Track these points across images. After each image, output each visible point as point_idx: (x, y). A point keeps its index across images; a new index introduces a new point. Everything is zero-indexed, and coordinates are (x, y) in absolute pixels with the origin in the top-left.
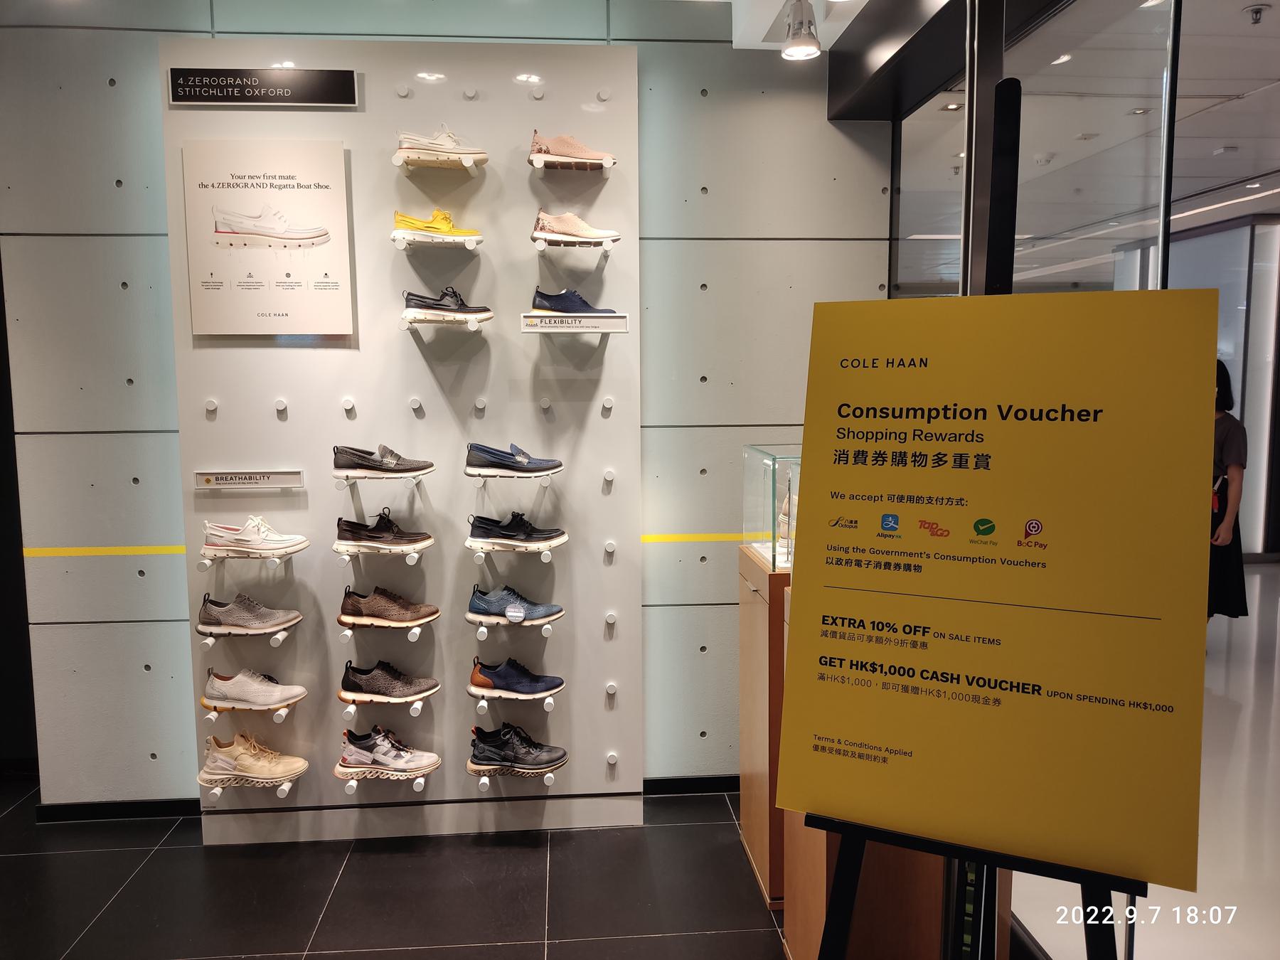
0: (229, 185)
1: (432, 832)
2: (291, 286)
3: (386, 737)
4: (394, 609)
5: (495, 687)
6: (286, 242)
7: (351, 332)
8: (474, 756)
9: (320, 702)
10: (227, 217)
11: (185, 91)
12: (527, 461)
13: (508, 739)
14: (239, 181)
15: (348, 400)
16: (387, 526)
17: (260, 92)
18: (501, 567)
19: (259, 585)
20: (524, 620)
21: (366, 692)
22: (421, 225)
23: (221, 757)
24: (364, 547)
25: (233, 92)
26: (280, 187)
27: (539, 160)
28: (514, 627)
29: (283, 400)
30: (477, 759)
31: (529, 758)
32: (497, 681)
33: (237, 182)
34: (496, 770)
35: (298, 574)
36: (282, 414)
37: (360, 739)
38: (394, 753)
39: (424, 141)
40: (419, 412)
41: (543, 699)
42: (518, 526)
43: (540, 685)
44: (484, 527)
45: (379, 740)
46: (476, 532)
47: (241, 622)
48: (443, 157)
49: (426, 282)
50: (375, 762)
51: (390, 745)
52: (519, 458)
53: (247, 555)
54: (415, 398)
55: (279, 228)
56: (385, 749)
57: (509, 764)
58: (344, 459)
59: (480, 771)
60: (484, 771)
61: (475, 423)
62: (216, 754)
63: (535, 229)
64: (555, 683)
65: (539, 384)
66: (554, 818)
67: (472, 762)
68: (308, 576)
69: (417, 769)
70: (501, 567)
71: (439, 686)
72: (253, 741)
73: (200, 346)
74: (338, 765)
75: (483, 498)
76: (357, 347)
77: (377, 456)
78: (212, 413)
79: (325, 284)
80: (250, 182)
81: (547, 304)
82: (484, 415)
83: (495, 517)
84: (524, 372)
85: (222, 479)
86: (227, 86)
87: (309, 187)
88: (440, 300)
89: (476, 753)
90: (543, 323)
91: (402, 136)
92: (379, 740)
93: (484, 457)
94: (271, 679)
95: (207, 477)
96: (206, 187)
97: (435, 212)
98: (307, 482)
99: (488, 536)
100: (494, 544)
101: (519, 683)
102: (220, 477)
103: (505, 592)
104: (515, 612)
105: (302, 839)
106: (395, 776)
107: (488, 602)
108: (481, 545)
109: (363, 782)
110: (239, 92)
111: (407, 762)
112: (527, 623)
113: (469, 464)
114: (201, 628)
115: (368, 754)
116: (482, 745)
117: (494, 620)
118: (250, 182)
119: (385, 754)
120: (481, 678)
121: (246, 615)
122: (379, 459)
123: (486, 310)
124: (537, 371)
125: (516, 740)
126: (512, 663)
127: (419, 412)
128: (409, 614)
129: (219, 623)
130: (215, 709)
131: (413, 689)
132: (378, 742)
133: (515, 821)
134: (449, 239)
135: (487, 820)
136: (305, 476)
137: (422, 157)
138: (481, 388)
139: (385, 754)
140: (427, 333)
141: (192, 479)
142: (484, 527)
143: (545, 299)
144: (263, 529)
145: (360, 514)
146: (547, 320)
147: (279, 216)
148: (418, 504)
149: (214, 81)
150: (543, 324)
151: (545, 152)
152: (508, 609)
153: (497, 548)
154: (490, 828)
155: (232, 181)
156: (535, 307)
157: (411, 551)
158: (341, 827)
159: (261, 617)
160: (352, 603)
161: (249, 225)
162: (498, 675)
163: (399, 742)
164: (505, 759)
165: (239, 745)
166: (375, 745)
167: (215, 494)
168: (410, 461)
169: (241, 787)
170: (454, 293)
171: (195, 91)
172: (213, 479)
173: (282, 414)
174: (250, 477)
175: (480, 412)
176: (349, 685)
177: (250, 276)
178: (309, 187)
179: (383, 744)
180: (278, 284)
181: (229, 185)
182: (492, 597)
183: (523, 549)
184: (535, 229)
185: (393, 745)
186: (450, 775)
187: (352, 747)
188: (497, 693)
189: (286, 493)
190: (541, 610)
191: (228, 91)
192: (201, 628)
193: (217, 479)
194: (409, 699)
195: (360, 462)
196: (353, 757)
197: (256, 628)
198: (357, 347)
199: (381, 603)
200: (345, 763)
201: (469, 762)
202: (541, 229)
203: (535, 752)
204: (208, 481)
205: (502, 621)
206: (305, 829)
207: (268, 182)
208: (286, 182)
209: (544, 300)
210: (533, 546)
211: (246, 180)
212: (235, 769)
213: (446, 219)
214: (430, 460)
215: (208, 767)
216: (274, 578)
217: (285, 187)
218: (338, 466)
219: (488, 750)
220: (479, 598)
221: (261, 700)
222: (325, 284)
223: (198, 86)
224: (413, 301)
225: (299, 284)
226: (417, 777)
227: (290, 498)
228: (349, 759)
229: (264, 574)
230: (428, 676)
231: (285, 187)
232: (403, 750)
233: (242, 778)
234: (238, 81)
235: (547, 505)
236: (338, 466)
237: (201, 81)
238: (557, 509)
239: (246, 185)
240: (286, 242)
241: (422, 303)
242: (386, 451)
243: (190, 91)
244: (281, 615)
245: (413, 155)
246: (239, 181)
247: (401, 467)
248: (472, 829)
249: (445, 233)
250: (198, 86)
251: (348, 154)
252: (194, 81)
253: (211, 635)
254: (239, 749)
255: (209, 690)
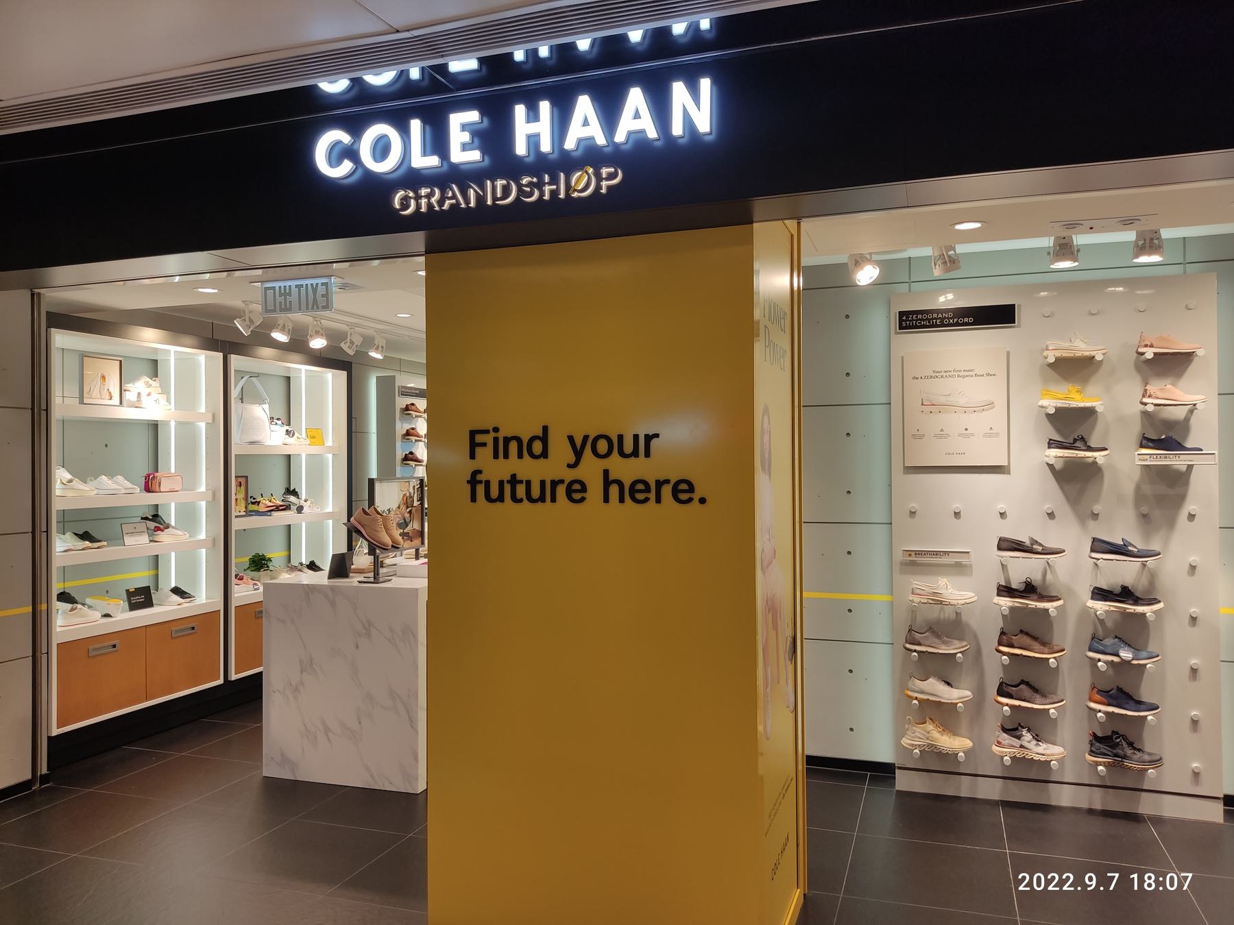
0: (931, 377)
1: (1053, 803)
2: (968, 436)
3: (1029, 731)
4: (1036, 646)
5: (1109, 705)
6: (966, 409)
7: (1007, 464)
8: (1091, 751)
9: (977, 704)
10: (929, 396)
11: (906, 324)
12: (1136, 550)
13: (1119, 742)
14: (937, 374)
15: (1002, 507)
16: (1029, 589)
17: (953, 321)
18: (1109, 624)
19: (938, 622)
20: (1133, 659)
21: (1016, 699)
22: (1061, 396)
23: (918, 730)
24: (1018, 602)
25: (936, 322)
26: (964, 377)
27: (1149, 354)
28: (1125, 663)
29: (957, 506)
30: (1092, 753)
31: (1135, 757)
32: (1104, 700)
33: (936, 375)
34: (1109, 762)
35: (964, 618)
36: (957, 515)
37: (1012, 730)
38: (1034, 742)
39: (1066, 345)
40: (1051, 515)
41: (1146, 716)
42: (1126, 594)
43: (1142, 707)
44: (1101, 594)
45: (1024, 732)
46: (1096, 596)
47: (933, 645)
48: (1079, 354)
49: (1058, 430)
50: (1022, 746)
51: (1031, 737)
52: (1130, 548)
53: (941, 602)
54: (1048, 507)
55: (962, 401)
56: (1029, 739)
57: (1120, 759)
58: (1005, 545)
59: (1097, 762)
60: (1100, 762)
61: (1091, 524)
62: (914, 728)
63: (1144, 396)
64: (1153, 707)
65: (1140, 497)
66: (1146, 806)
67: (1089, 754)
68: (972, 621)
69: (1053, 755)
70: (1109, 624)
71: (1064, 702)
72: (937, 722)
73: (908, 473)
74: (994, 746)
75: (1096, 575)
76: (1009, 473)
77: (1028, 543)
78: (913, 513)
79: (991, 434)
80: (944, 374)
81: (1150, 444)
82: (1097, 519)
83: (1105, 588)
84: (1129, 489)
85: (919, 554)
86: (933, 319)
87: (982, 375)
88: (1074, 443)
89: (1093, 749)
90: (1152, 459)
91: (1048, 343)
92: (1024, 732)
93: (1100, 546)
94: (948, 684)
95: (909, 553)
96: (917, 378)
97: (1071, 388)
98: (973, 559)
99: (1106, 601)
100: (1110, 606)
101: (1127, 703)
102: (918, 553)
103: (1116, 640)
104: (1126, 654)
105: (962, 796)
106: (1037, 757)
107: (1105, 646)
108: (1101, 607)
109: (1014, 758)
110: (940, 322)
111: (1044, 749)
112: (1134, 662)
113: (1092, 550)
114: (908, 646)
115: (1017, 740)
116: (1098, 744)
117: (1110, 658)
118: (944, 374)
119: (1029, 742)
120: (1098, 697)
121: (937, 640)
122: (1029, 545)
123: (1106, 449)
124: (1138, 488)
125: (1124, 743)
126: (1120, 690)
127: (1051, 515)
128: (1046, 650)
129: (920, 644)
130: (916, 698)
131: (1048, 701)
132: (1024, 733)
133: (1117, 803)
134: (1082, 405)
135: (1097, 799)
136: (972, 554)
137: (1064, 355)
138: (1097, 500)
139: (1029, 742)
140: (1059, 465)
141: (901, 553)
142: (1101, 594)
143: (1150, 442)
144: (949, 587)
145: (1008, 580)
146: (1155, 456)
147: (962, 393)
148: (1049, 577)
149: (925, 316)
150: (1152, 459)
151: (1150, 346)
152: (1121, 651)
153: (1112, 609)
154: (1098, 806)
155: (933, 375)
156: (1142, 446)
157: (1050, 606)
158: (990, 790)
159: (945, 643)
160: (1005, 638)
161: (942, 400)
162: (1111, 697)
163: (1037, 736)
164: (1116, 755)
165: (930, 724)
166: (1022, 736)
167: (913, 563)
168: (1049, 548)
169: (933, 752)
170: (1082, 438)
171: (913, 323)
172: (913, 554)
173: (957, 515)
174: (937, 553)
175: (1095, 516)
176: (1001, 692)
177: (942, 430)
178: (982, 375)
179: (1027, 736)
180: (960, 435)
181: (931, 377)
182: (1109, 642)
183: (1132, 611)
184: (1144, 396)
185: (1033, 736)
186: (1068, 765)
187: (1005, 735)
188: (1111, 709)
189: (958, 565)
190: (1144, 654)
191: (933, 322)
192: (908, 646)
193: (916, 554)
194: (1047, 707)
195: (1017, 547)
196: (1007, 741)
197: (943, 650)
198: (1009, 473)
199: (1027, 640)
200: (999, 744)
201: (1087, 756)
202: (1149, 397)
203: (1139, 754)
204: (910, 555)
205: (1116, 659)
206: (964, 788)
207: (956, 374)
208: (968, 373)
209: (1146, 442)
210: (1140, 609)
211: (942, 374)
212: (928, 739)
213: (1078, 391)
214: (1062, 547)
215: (908, 735)
216: (949, 620)
217: (967, 376)
218: (999, 548)
219: (1103, 748)
220: (1098, 643)
221: (946, 696)
222: (991, 434)
223: (914, 320)
224: (1052, 444)
225: (973, 435)
226: (1052, 760)
227: (960, 568)
228: (1003, 742)
229: (942, 616)
230: (1054, 693)
231: (967, 376)
232: (1040, 741)
233: (933, 745)
234: (940, 316)
235: (1144, 581)
236: (999, 548)
237: (917, 317)
238: (1152, 584)
239: (942, 377)
240: (966, 409)
241: (1061, 446)
242: (1034, 542)
243: (909, 324)
244: (957, 643)
245: (1058, 354)
246: (937, 374)
247: (1046, 552)
248: (1084, 805)
249: (1078, 400)
250: (914, 320)
251: (1008, 353)
252: (912, 317)
253: (915, 651)
254: (930, 726)
255: (910, 685)
